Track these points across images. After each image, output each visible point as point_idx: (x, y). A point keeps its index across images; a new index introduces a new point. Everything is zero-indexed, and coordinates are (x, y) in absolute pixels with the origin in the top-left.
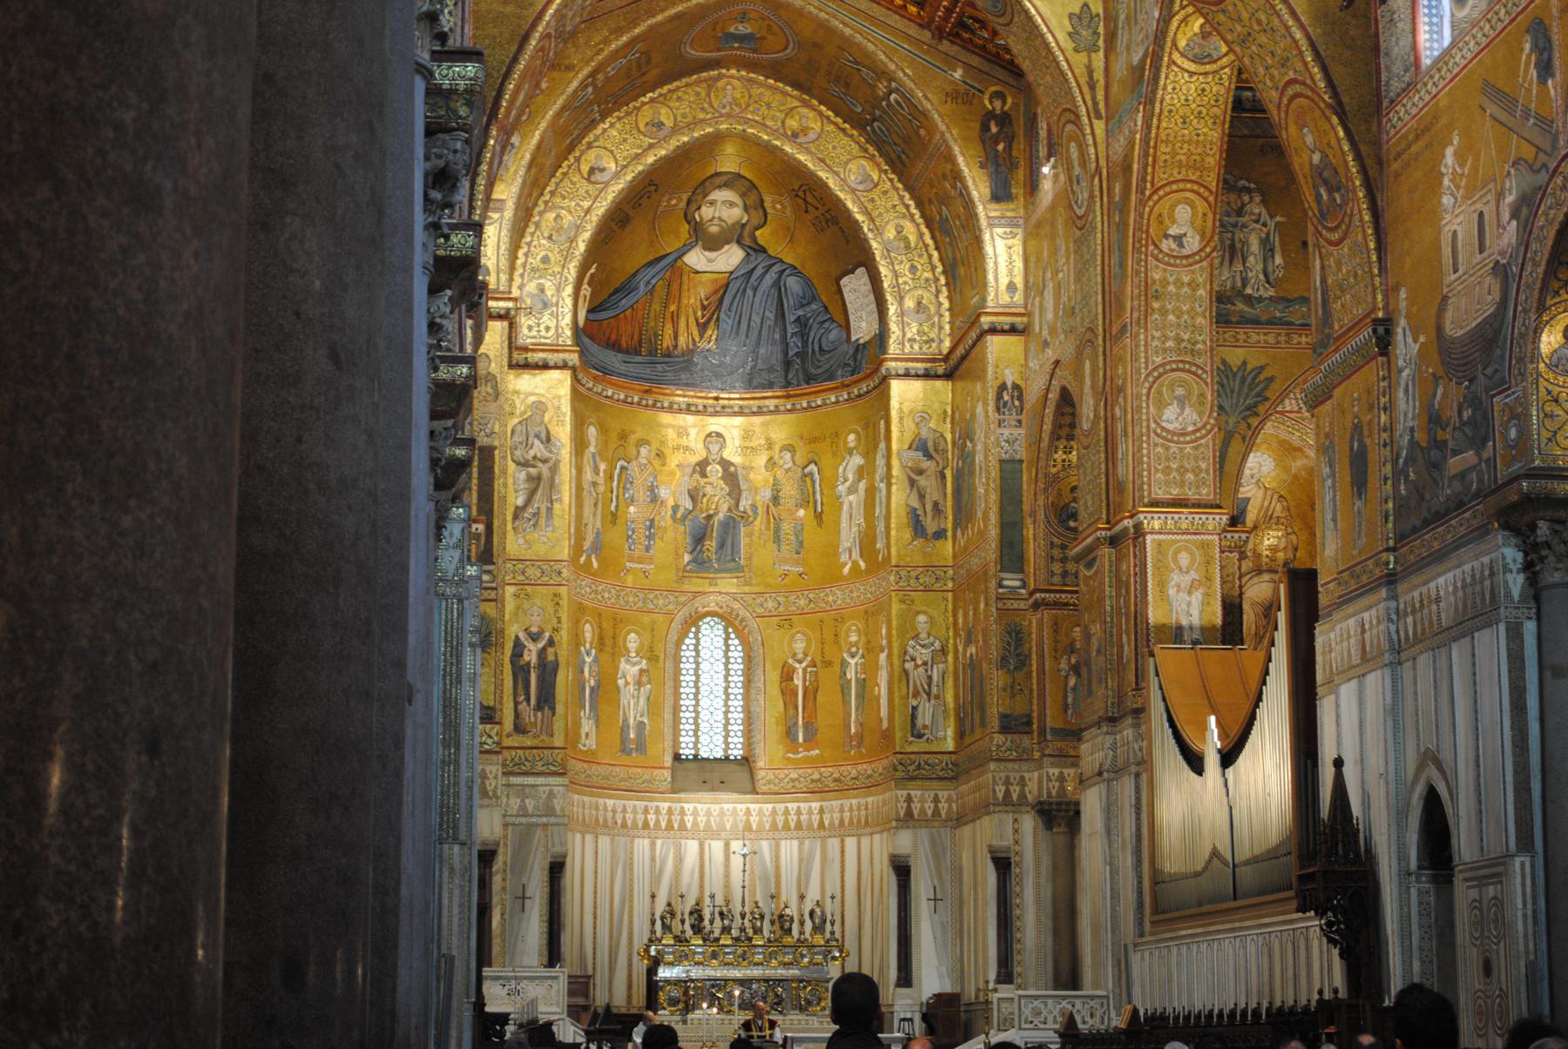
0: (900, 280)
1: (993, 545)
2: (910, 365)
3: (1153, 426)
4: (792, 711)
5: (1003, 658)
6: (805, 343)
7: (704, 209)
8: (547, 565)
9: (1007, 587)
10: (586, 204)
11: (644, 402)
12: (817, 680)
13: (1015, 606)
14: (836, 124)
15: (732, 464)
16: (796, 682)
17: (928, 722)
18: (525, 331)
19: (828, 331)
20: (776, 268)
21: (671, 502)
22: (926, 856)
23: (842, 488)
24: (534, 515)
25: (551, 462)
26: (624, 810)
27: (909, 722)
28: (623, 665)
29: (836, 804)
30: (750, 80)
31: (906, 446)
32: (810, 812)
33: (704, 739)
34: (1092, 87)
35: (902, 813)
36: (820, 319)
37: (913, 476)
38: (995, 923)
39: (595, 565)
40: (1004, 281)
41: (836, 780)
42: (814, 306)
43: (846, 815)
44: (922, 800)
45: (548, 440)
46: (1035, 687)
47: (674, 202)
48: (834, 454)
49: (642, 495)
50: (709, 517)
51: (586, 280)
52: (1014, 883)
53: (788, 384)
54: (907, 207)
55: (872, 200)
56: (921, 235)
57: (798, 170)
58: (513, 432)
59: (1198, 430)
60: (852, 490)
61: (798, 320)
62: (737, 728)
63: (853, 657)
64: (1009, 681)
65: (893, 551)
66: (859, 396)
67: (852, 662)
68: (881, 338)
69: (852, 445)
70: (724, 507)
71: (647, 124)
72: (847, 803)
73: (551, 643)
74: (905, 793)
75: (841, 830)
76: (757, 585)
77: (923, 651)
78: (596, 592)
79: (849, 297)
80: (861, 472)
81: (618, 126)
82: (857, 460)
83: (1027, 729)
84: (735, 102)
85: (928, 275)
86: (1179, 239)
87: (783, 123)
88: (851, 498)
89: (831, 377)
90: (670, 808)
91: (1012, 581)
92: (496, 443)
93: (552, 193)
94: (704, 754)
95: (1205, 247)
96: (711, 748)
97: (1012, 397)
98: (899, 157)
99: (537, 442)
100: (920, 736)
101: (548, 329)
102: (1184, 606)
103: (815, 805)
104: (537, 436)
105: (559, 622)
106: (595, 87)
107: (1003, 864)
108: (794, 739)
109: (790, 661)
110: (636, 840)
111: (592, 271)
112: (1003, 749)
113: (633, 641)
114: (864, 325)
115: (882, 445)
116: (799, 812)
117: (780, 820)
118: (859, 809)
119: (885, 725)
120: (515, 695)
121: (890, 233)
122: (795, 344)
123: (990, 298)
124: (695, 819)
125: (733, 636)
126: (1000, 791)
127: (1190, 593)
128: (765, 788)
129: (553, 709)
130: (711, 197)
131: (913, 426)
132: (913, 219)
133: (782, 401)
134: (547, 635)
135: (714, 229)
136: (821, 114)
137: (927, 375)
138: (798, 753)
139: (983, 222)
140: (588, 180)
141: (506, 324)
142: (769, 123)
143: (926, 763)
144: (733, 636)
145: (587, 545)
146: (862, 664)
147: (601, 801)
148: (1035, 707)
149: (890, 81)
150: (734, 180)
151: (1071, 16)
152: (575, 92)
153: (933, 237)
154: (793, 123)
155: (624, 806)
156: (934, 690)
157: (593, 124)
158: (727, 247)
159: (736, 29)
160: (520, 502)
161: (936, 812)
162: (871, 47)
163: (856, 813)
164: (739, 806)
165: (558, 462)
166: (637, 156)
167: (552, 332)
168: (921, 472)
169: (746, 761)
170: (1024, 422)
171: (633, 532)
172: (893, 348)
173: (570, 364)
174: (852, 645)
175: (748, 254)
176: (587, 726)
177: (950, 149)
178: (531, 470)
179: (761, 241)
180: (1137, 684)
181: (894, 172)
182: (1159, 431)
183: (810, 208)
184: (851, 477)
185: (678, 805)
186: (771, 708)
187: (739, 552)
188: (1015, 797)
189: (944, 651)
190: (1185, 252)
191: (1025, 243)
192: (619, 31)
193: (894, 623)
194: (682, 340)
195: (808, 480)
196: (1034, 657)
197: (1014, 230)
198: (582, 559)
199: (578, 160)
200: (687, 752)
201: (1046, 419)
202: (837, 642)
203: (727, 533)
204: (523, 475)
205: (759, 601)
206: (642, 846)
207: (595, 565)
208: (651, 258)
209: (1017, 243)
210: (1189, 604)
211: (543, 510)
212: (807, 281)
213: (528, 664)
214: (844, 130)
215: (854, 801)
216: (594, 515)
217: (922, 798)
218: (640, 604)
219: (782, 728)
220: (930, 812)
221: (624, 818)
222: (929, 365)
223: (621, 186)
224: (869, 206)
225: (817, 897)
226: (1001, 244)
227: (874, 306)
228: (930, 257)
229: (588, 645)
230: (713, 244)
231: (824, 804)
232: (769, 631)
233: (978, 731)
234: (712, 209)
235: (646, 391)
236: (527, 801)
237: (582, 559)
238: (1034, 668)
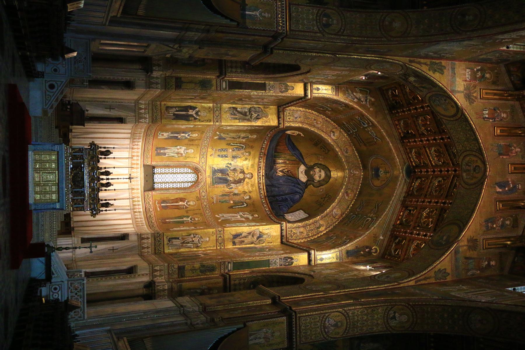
0: (308, 226)
1: (242, 259)
2: (285, 230)
3: (327, 315)
4: (171, 202)
5: (204, 265)
6: (280, 201)
7: (318, 169)
8: (219, 118)
9: (228, 265)
10: (324, 130)
11: (261, 154)
12: (181, 209)
13: (222, 268)
14: (350, 205)
15: (244, 181)
16: (180, 203)
17: (174, 243)
18: (288, 112)
19: (285, 208)
20: (301, 192)
21: (232, 163)
22: (128, 246)
23: (241, 213)
24: (235, 114)
25: (251, 119)
26: (138, 149)
27: (174, 237)
28: (184, 148)
29: (143, 216)
30: (360, 179)
31: (261, 231)
32: (139, 209)
33: (160, 176)
34: (425, 279)
35: (143, 236)
36: (288, 205)
37: (251, 234)
38: (108, 270)
39: (215, 138)
40: (323, 257)
41: (150, 216)
42: (291, 203)
43: (139, 220)
44: (147, 243)
45: (257, 118)
46: (195, 278)
47: (321, 160)
48: (251, 211)
49: (234, 153)
50: (228, 174)
51: (300, 133)
52: (124, 276)
53: (268, 196)
54: (329, 227)
55: (330, 217)
56: (321, 232)
57: (336, 194)
58: (259, 107)
59: (326, 333)
60: (241, 216)
61: (287, 199)
62: (163, 186)
63: (190, 219)
64: (196, 268)
65: (228, 228)
66: (270, 217)
67: (189, 219)
68: (289, 222)
69: (255, 216)
70: (231, 179)
71: (347, 148)
72: (143, 219)
73: (195, 119)
74: (150, 237)
75: (134, 218)
76: (209, 190)
77: (197, 240)
78: (207, 138)
79: (297, 212)
80: (247, 219)
81: (346, 140)
82: (251, 218)
83: (180, 276)
84: (354, 174)
85: (310, 235)
86: (394, 318)
87: (349, 189)
88: (239, 216)
89: (272, 209)
90: (138, 164)
91: (230, 266)
92: (267, 92)
93: (327, 120)
94: (155, 176)
95: (391, 328)
96: (157, 178)
97: (289, 262)
98: (345, 223)
99: (257, 115)
100: (169, 241)
101: (289, 119)
102: (259, 336)
103: (141, 210)
104: (258, 115)
105: (202, 121)
106: (366, 128)
107: (131, 271)
108: (162, 203)
109: (187, 201)
110: (128, 153)
111: (302, 135)
112: (173, 268)
113: (191, 151)
114: (290, 217)
115: (258, 224)
116: (139, 205)
117: (136, 199)
118: (141, 223)
119: (171, 230)
120: (178, 107)
121: (321, 222)
122: (280, 198)
123: (318, 252)
124: (135, 172)
125: (192, 184)
126: (157, 268)
127: (264, 338)
128: (146, 194)
129: (174, 119)
130: (322, 171)
131: (266, 232)
132: (326, 229)
133: (264, 195)
134: (198, 117)
135: (312, 173)
136: (352, 200)
137: (282, 236)
138: (158, 204)
139: (340, 249)
140: (331, 131)
141: (303, 95)
142: (349, 184)
143: (160, 243)
144: (192, 184)
145: (222, 135)
146: (189, 222)
147: (141, 140)
148: (188, 278)
149: (376, 217)
150: (328, 176)
151: (445, 269)
152: (369, 119)
153: (321, 236)
154: (349, 192)
155: (139, 149)
156: (185, 245)
157: (347, 131)
158: (306, 177)
159: (381, 171)
160: (238, 109)
161: (144, 248)
162: (387, 210)
163: (140, 222)
164: (140, 186)
165: (251, 121)
166: (338, 146)
167: (289, 120)
168: (253, 236)
169: (153, 189)
170: (281, 267)
171: (224, 151)
172: (289, 225)
173: (280, 125)
174: (194, 219)
175: (304, 183)
176: (166, 135)
177: (360, 236)
178: (248, 113)
179: (309, 187)
180: (225, 319)
181: (338, 223)
182: (325, 317)
183: (323, 199)
184: (245, 216)
185: (139, 167)
186: (173, 195)
187: (218, 184)
188: (156, 273)
189: (197, 247)
190: (389, 320)
191: (335, 262)
192: (387, 132)
193: (205, 230)
194: (278, 165)
195: (242, 204)
196: (205, 276)
197: (339, 259)
198: (218, 133)
199: (336, 128)
200: (156, 170)
201: (287, 274)
202: (194, 214)
203: (224, 180)
204: (246, 110)
205: (204, 190)
206: (126, 154)
207: (215, 138)
208: (303, 154)
209: (334, 260)
210: (260, 338)
211: (236, 117)
212: (298, 201)
213: (189, 112)
214: (348, 207)
215: (144, 222)
216: (230, 137)
217: (148, 243)
218: (202, 153)
219: (165, 199)
220: (143, 246)
221: (136, 149)
222: (285, 236)
223: (330, 141)
224: (329, 216)
225: (115, 205)
226: (330, 256)
227: (297, 220)
228: (315, 235)
229: (191, 135)
230: (307, 173)
231: (142, 213)
232: (195, 194)
233: (175, 259)
234: (318, 171)
235: (265, 154)
236: (143, 110)
237: (218, 133)
238: (202, 277)
